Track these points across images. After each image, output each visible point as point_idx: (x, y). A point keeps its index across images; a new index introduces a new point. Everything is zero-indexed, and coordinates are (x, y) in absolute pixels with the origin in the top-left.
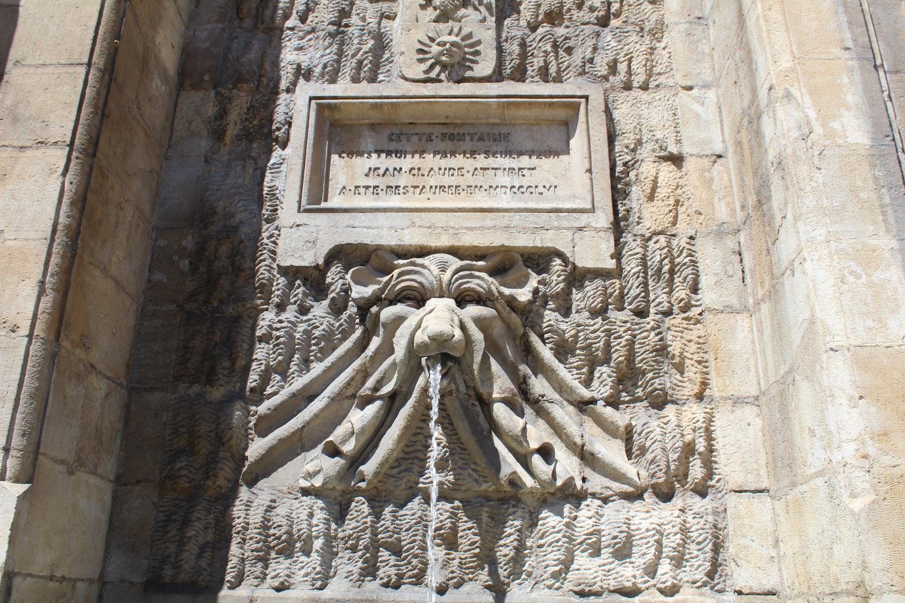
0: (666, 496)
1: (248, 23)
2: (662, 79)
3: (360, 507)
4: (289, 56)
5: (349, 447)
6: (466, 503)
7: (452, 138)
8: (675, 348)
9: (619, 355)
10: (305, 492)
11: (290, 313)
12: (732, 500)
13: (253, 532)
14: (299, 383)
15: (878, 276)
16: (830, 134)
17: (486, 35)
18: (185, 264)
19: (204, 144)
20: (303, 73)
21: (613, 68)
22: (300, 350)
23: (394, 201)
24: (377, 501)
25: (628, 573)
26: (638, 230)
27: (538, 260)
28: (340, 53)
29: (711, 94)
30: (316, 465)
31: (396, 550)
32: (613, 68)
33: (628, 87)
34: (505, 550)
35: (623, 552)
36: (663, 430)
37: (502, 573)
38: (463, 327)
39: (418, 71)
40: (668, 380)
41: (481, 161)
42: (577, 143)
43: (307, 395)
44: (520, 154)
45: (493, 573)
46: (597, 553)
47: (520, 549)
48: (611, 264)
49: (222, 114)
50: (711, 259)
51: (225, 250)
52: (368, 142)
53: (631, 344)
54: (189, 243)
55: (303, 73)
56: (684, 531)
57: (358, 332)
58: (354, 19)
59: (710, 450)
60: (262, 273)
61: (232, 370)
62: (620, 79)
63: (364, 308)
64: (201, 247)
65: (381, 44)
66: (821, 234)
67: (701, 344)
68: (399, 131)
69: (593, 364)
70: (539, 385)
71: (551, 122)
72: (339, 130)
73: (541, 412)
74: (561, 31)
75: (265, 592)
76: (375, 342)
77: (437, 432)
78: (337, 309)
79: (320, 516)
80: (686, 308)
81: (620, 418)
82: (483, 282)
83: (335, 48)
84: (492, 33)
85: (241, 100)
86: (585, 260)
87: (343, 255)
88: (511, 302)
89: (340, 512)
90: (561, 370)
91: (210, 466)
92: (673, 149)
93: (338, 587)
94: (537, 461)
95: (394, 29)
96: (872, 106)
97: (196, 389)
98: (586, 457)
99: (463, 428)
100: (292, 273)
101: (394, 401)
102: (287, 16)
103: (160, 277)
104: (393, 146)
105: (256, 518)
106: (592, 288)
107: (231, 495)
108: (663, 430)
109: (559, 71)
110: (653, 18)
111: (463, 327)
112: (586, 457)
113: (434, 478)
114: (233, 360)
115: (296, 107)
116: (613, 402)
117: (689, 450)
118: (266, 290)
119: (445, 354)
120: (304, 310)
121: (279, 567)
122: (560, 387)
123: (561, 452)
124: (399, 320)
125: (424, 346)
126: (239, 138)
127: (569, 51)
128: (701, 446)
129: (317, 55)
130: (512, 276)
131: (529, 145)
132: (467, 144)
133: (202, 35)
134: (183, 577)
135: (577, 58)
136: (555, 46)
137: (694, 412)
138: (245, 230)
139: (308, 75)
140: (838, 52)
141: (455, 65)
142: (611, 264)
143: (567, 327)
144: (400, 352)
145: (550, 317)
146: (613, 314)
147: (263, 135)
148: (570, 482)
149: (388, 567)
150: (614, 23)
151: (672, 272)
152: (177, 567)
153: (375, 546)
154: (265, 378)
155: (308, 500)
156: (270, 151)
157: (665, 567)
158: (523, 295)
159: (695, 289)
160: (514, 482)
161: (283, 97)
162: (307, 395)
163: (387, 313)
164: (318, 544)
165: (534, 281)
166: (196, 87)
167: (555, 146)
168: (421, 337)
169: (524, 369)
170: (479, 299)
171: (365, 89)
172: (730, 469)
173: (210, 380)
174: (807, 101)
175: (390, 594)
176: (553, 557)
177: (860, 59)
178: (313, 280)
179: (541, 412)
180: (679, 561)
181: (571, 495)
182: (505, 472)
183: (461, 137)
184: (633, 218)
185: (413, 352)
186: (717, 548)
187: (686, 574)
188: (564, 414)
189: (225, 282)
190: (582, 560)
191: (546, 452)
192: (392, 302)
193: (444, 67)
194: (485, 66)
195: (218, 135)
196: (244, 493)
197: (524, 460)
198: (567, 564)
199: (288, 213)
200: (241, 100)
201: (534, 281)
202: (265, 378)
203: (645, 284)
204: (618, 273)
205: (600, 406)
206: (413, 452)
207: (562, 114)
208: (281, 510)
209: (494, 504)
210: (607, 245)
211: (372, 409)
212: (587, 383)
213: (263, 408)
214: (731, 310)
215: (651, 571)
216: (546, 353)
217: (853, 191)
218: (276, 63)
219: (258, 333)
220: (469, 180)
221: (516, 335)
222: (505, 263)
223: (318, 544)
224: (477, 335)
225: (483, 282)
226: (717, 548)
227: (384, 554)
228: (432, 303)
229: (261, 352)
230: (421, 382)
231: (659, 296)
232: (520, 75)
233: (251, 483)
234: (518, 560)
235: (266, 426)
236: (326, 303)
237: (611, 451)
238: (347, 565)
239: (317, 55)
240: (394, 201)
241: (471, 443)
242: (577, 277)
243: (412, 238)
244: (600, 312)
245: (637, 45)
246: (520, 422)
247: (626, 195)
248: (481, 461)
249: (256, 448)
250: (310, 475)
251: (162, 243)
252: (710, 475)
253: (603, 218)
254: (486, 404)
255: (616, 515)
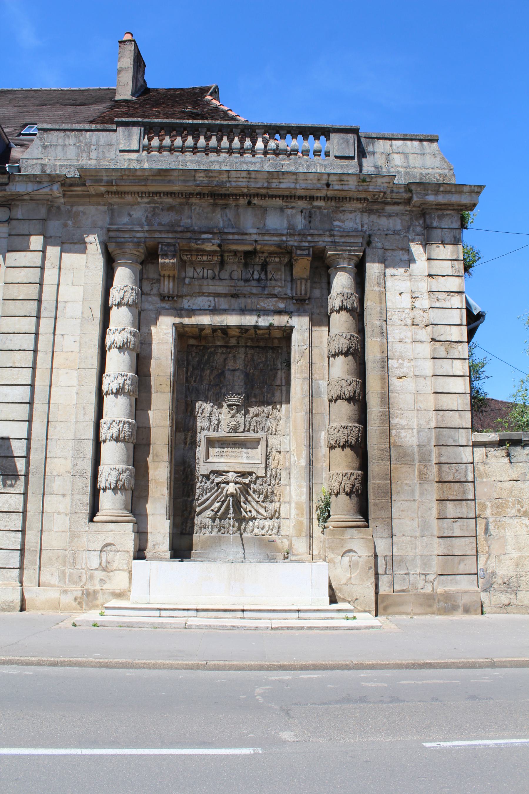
0: (271, 519)
1: (189, 414)
2: (279, 432)
3: (217, 520)
4: (199, 424)
5: (216, 510)
6: (236, 520)
7: (234, 444)
8: (275, 492)
9: (264, 493)
10: (208, 518)
11: (203, 484)
12: (282, 520)
13: (199, 524)
14: (205, 497)
15: (302, 489)
16: (299, 463)
17: (242, 421)
18: (181, 473)
19: (183, 446)
20: (202, 429)
21: (269, 429)
22: (205, 491)
23: (222, 460)
24: (220, 519)
25: (263, 532)
26: (271, 467)
27: (250, 474)
28: (210, 424)
29: (288, 437)
30: (209, 513)
31: (224, 528)
32: (269, 429)
33: (271, 434)
34: (243, 527)
35: (263, 528)
36: (271, 507)
37: (242, 531)
38: (236, 490)
39: (227, 430)
40: (273, 498)
41: (240, 450)
42: (260, 447)
43: (207, 500)
44: (248, 448)
45: (241, 532)
46: (258, 528)
47: (245, 527)
48: (264, 475)
49: (186, 438)
50: (284, 474)
51: (189, 470)
52: (217, 445)
53: (267, 491)
54: (182, 468)
55: (202, 429)
56: (274, 525)
57: (216, 488)
58: (213, 415)
59: (280, 511)
60: (197, 476)
61: (192, 494)
62: (271, 432)
63: (218, 484)
64: (184, 469)
65: (219, 421)
66: (294, 481)
67: (280, 492)
68: (223, 443)
69: (260, 494)
70: (250, 498)
71: (255, 441)
72: (211, 442)
73: (250, 503)
74: (258, 419)
75: (201, 534)
76: (220, 490)
77: (231, 508)
78: (212, 483)
79: (210, 522)
80: (278, 484)
81: (264, 505)
82: (240, 479)
83: (209, 422)
84: (243, 421)
85: (190, 435)
86: (259, 475)
87: (213, 472)
88: (245, 483)
89: (214, 521)
90: (254, 495)
91: (190, 513)
92: (279, 450)
93: (214, 534)
94: (248, 513)
95: (222, 417)
96: (307, 457)
97: (186, 498)
98: (258, 512)
99: (236, 507)
100: (203, 476)
101: (223, 502)
102: (198, 413)
103: (177, 476)
104: (222, 446)
105: (199, 522)
106: (260, 480)
107: (194, 518)
108: (271, 507)
109: (257, 431)
110: (279, 416)
111: (236, 490)
112: (258, 512)
113: (231, 515)
114: (193, 493)
115: (201, 437)
116: (263, 502)
117: (276, 511)
118: (198, 479)
119: (232, 495)
120: (206, 483)
121: (203, 530)
122: (253, 499)
123: (253, 511)
124: (224, 487)
125: (229, 494)
126: (190, 444)
127: (260, 424)
128: (278, 510)
129: (206, 424)
130: (245, 476)
131: (250, 446)
132: (237, 446)
133: (180, 418)
134: (187, 532)
135: (261, 427)
136: (257, 423)
137: (277, 504)
138: (193, 465)
139: (203, 429)
140: (303, 446)
141: (235, 429)
142: (264, 475)
143: (255, 487)
144: (224, 493)
145: (252, 485)
146: (264, 485)
147: (194, 444)
148: (254, 516)
149: (222, 530)
150: (270, 417)
151: (276, 477)
152: (186, 530)
153: (220, 527)
154: (199, 496)
155: (208, 519)
156: (196, 447)
157: (270, 531)
158: (247, 481)
159: (280, 480)
160: (244, 516)
161: (198, 434)
162: (207, 500)
163: (222, 486)
164: (210, 527)
165: (249, 478)
166: (180, 431)
167: (256, 447)
168: (228, 492)
169: (247, 496)
170: (239, 483)
171: (215, 434)
172: (282, 515)
173: (189, 496)
174: (296, 457)
175: (223, 535)
176: (251, 529)
177: (307, 447)
178: (207, 477)
179: (250, 503)
180: (272, 530)
181: (254, 518)
182: (243, 515)
183: (236, 444)
184: (270, 464)
185: (227, 496)
186: (279, 528)
187: (273, 533)
188: (254, 504)
189: (190, 477)
190: (256, 530)
191: (250, 511)
192: (223, 483)
193: (233, 429)
194: (241, 429)
195: (185, 443)
196: (196, 518)
197: (246, 512)
198: (253, 530)
199: (201, 462)
200: (190, 435)
201: (250, 477)
202: (199, 496)
203: (271, 479)
204: (266, 477)
205: (261, 503)
206: (227, 511)
207: (257, 440)
208: (203, 521)
209: (241, 520)
210: (264, 471)
211: (220, 503)
212: (259, 498)
213: (199, 502)
214: (286, 485)
215: (267, 532)
216: (251, 492)
217: (301, 474)
218: (196, 426)
219: (197, 487)
220: (238, 454)
221: (245, 489)
222: (244, 474)
223: (210, 527)
224: (238, 491)
225: (240, 479)
226: (279, 528)
227: (222, 528)
228: (230, 484)
229: (197, 491)
230: (228, 499)
231: (273, 482)
232: (249, 431)
233: (198, 515)
234: (245, 529)
235: (200, 505)
236: (210, 481)
237: (262, 511)
238: (215, 530)
239: (206, 424)
240: (222, 460)
241: (237, 509)
242: (258, 478)
243: (226, 469)
244: (262, 485)
245: (274, 424)
246: (246, 506)
247: (269, 459)
248: (239, 513)
249: (198, 509)
250: (209, 515)
251: (176, 468)
252: (279, 515)
253: (263, 465)
254: (240, 502)
255: (262, 522)
